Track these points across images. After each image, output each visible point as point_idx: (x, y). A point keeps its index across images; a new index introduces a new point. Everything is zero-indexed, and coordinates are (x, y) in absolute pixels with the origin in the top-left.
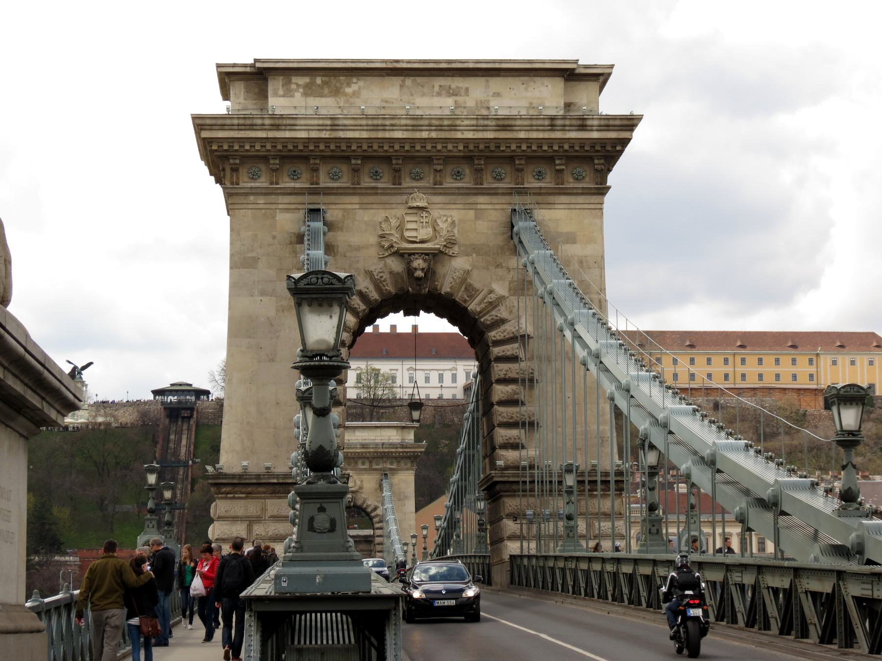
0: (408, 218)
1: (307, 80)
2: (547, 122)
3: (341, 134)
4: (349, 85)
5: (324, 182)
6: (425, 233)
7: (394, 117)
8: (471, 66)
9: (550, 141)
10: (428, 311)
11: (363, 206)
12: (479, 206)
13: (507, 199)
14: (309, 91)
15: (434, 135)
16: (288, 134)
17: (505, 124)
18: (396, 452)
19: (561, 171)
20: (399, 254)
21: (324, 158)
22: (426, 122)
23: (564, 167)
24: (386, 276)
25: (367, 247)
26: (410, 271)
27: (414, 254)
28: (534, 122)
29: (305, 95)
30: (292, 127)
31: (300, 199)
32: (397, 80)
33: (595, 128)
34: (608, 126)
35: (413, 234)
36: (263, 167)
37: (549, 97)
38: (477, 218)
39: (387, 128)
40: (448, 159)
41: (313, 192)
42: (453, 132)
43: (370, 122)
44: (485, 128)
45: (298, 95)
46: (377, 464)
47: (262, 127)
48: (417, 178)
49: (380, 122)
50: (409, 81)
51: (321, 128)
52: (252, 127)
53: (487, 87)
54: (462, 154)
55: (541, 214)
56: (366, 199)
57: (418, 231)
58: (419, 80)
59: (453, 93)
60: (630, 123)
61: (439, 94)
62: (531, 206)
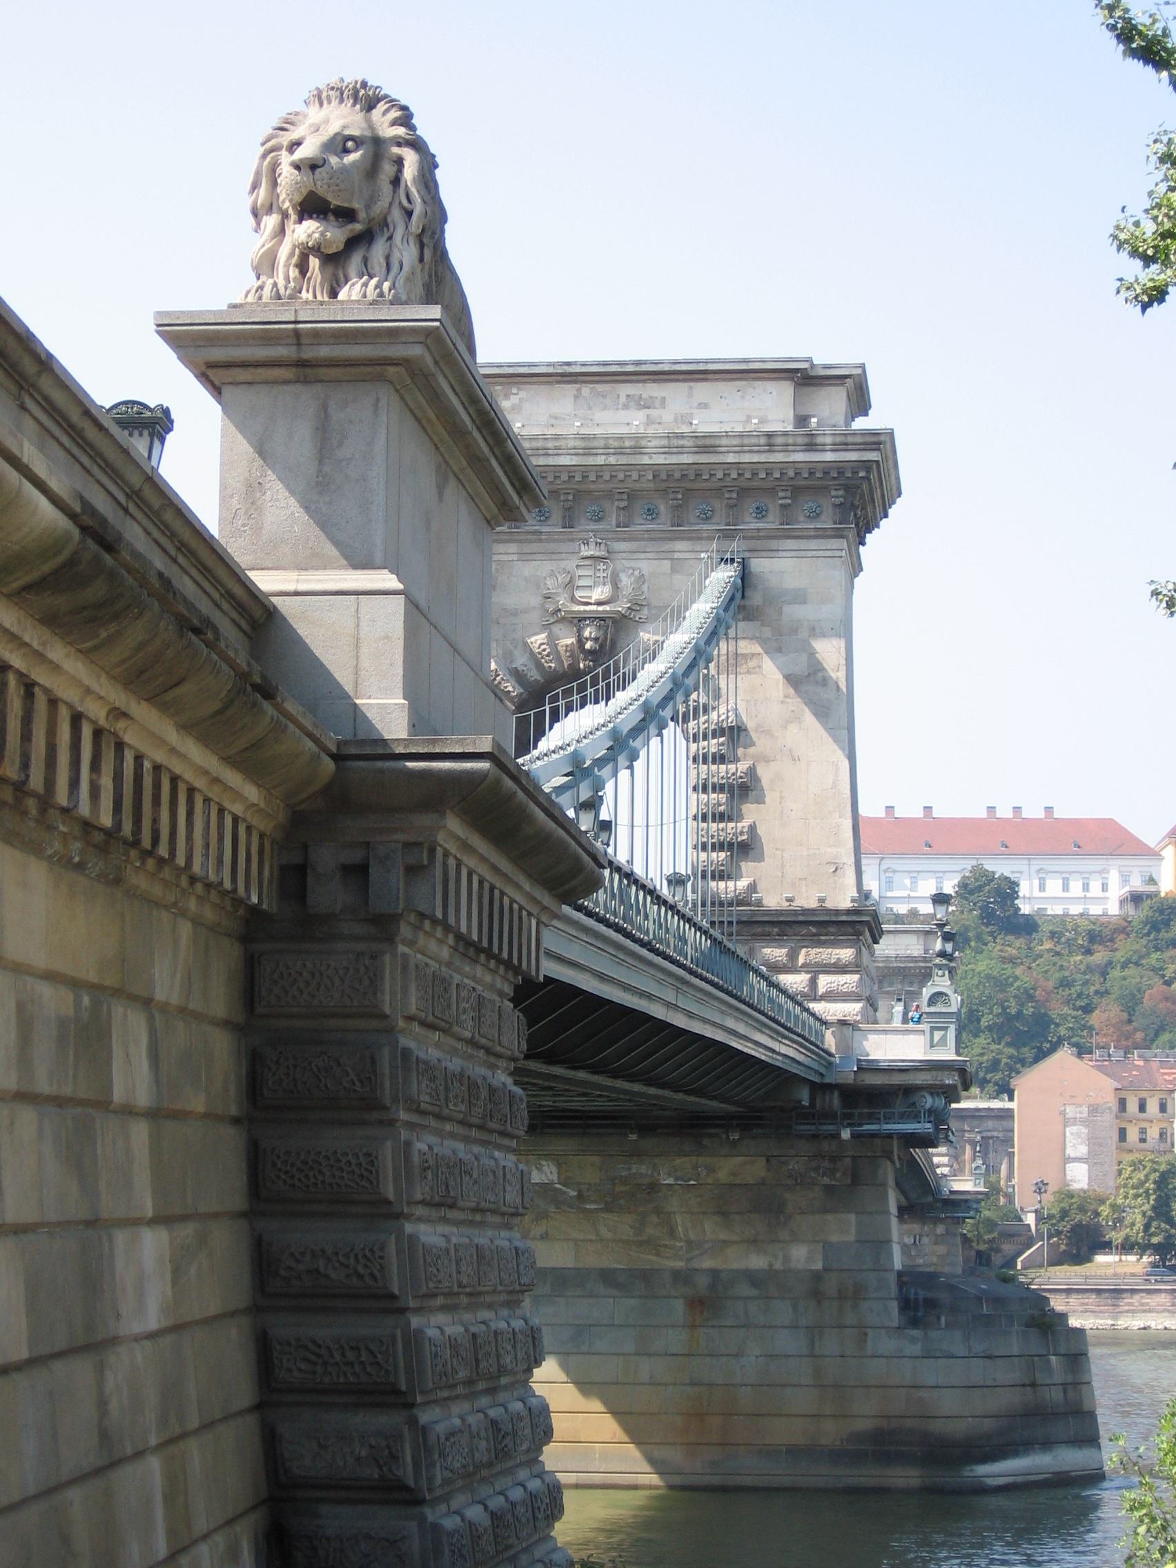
0: (581, 572)
2: (763, 441)
4: (507, 396)
7: (557, 437)
8: (666, 368)
9: (769, 468)
11: (524, 557)
12: (676, 555)
15: (612, 460)
17: (706, 444)
18: (914, 968)
23: (789, 501)
25: (526, 611)
27: (585, 619)
28: (746, 441)
32: (571, 389)
33: (828, 447)
34: (846, 444)
37: (772, 409)
38: (674, 570)
39: (550, 452)
40: (632, 496)
42: (637, 456)
44: (680, 450)
46: (891, 985)
49: (540, 444)
50: (586, 390)
53: (690, 396)
54: (651, 485)
56: (527, 548)
59: (644, 404)
61: (626, 407)
62: (747, 555)
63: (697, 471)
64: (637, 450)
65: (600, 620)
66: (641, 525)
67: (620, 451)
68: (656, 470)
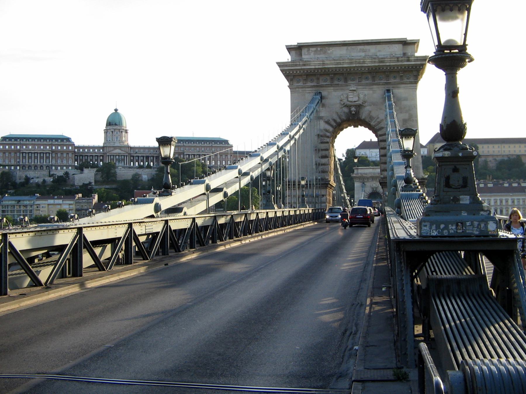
0: (349, 94)
2: (396, 59)
3: (326, 66)
4: (329, 50)
5: (322, 83)
6: (356, 99)
10: (361, 125)
11: (335, 90)
13: (383, 86)
15: (357, 65)
19: (401, 76)
20: (346, 106)
21: (321, 75)
22: (354, 61)
24: (342, 114)
26: (350, 112)
29: (315, 54)
30: (309, 65)
31: (314, 89)
32: (345, 48)
35: (351, 99)
36: (301, 78)
40: (363, 73)
41: (317, 86)
43: (335, 62)
44: (375, 62)
45: (312, 54)
47: (299, 65)
48: (353, 80)
50: (349, 48)
51: (319, 65)
52: (296, 65)
55: (396, 91)
57: (353, 98)
59: (364, 51)
61: (360, 52)
64: (364, 63)
65: (355, 106)
66: (364, 82)
67: (359, 63)
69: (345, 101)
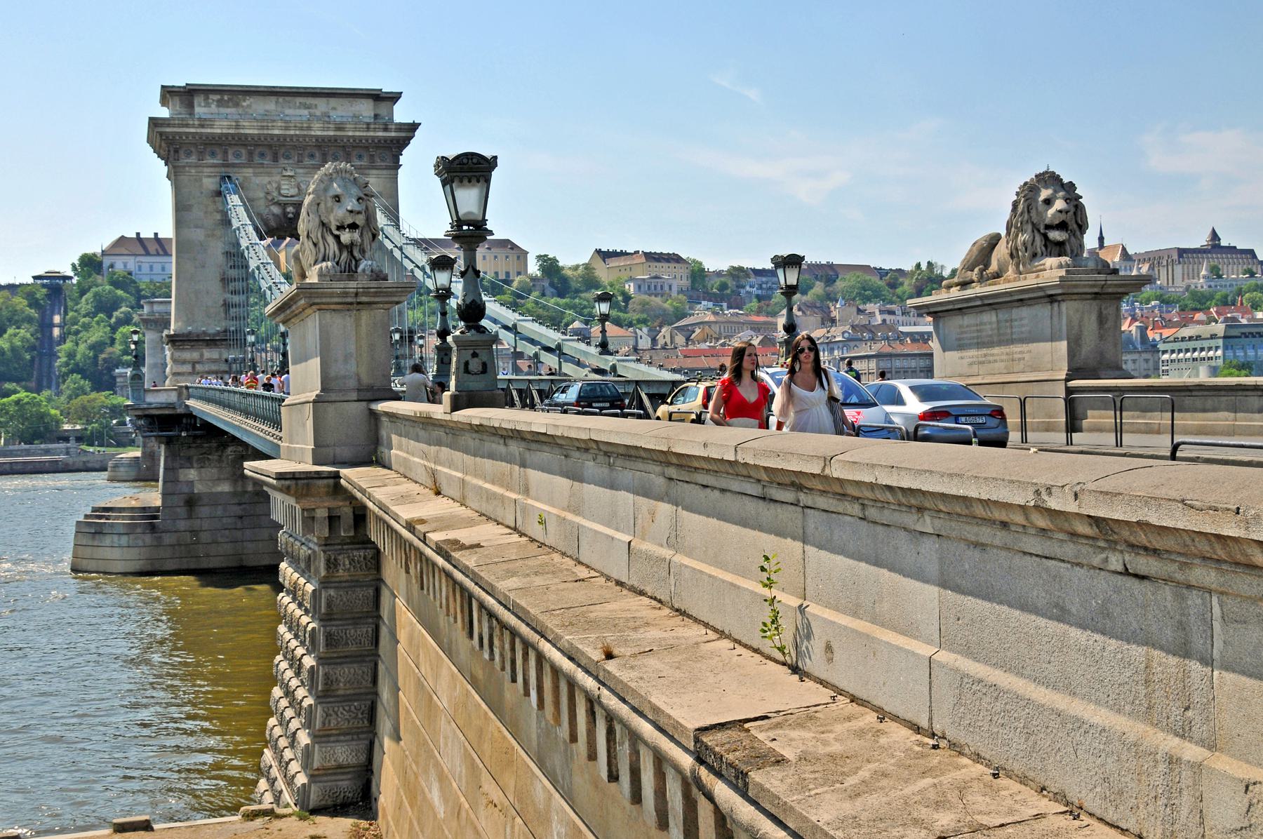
1: (217, 97)
5: (232, 159)
9: (367, 138)
14: (220, 103)
16: (209, 131)
17: (339, 128)
20: (278, 204)
21: (230, 145)
24: (270, 217)
26: (285, 214)
29: (218, 106)
30: (211, 126)
31: (217, 170)
32: (273, 99)
41: (223, 165)
47: (193, 126)
48: (288, 158)
50: (281, 99)
58: (288, 99)
60: (414, 127)
63: (334, 140)
65: (293, 204)
67: (301, 129)
68: (317, 137)
69: (275, 194)
